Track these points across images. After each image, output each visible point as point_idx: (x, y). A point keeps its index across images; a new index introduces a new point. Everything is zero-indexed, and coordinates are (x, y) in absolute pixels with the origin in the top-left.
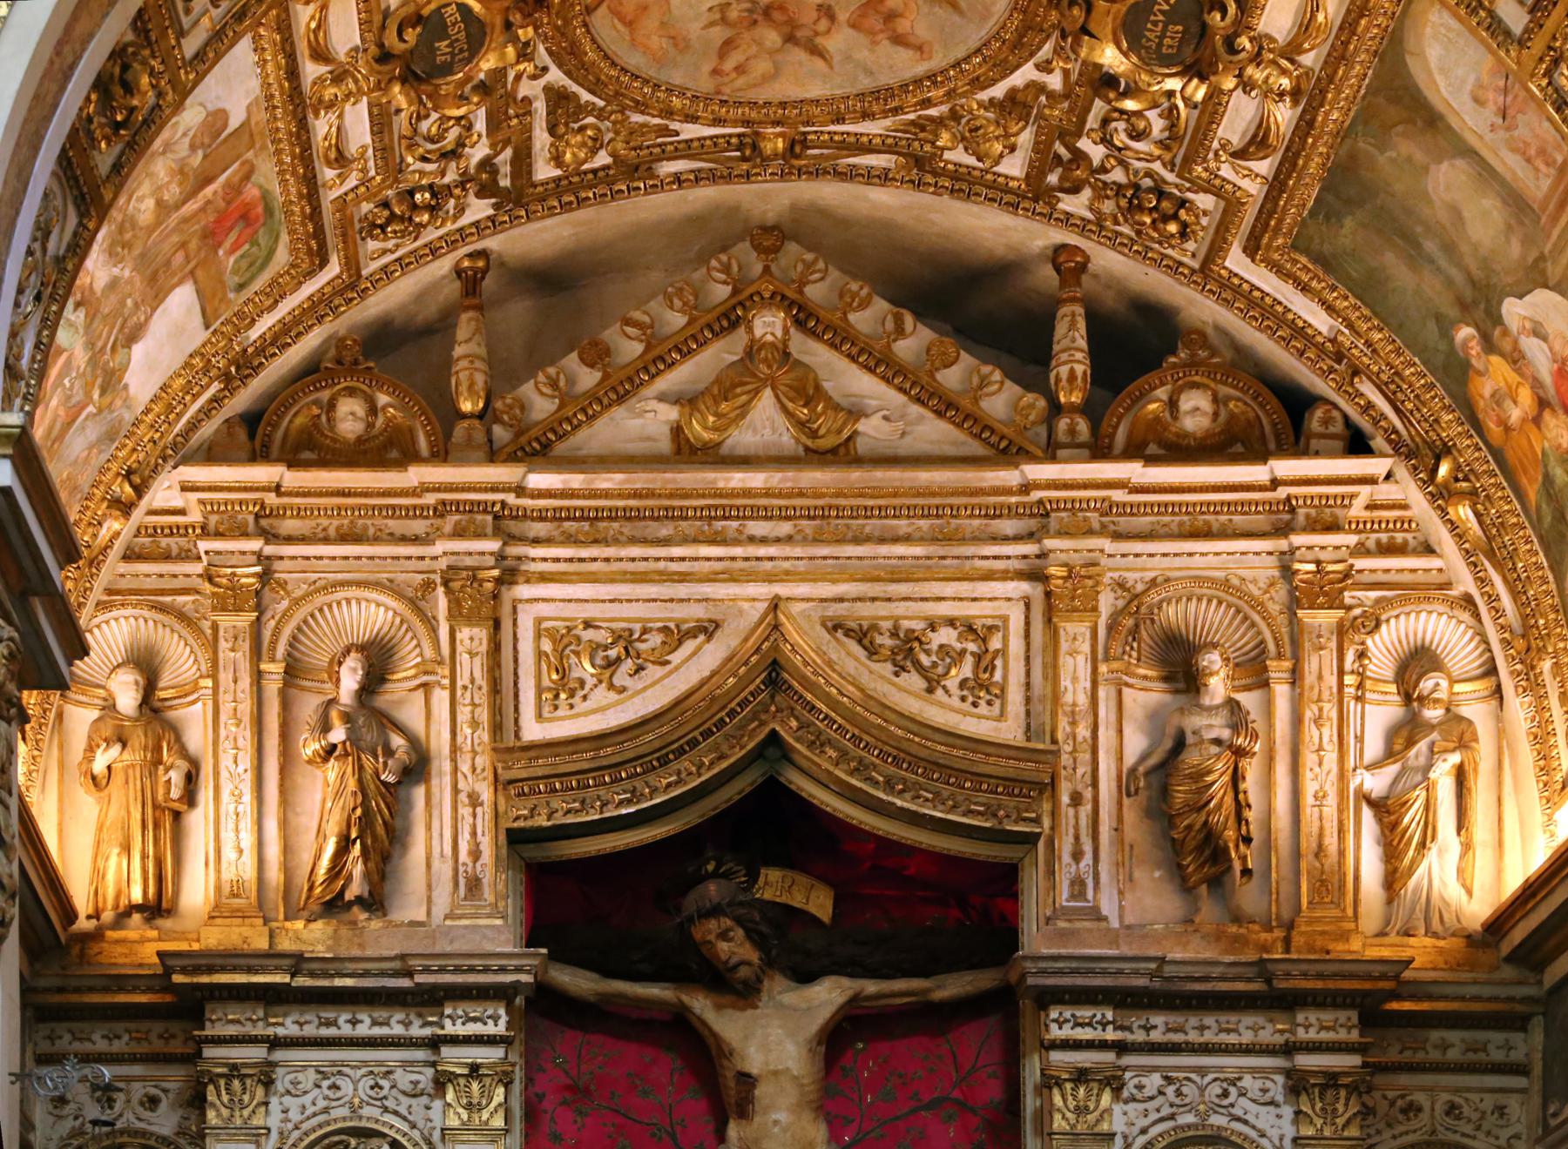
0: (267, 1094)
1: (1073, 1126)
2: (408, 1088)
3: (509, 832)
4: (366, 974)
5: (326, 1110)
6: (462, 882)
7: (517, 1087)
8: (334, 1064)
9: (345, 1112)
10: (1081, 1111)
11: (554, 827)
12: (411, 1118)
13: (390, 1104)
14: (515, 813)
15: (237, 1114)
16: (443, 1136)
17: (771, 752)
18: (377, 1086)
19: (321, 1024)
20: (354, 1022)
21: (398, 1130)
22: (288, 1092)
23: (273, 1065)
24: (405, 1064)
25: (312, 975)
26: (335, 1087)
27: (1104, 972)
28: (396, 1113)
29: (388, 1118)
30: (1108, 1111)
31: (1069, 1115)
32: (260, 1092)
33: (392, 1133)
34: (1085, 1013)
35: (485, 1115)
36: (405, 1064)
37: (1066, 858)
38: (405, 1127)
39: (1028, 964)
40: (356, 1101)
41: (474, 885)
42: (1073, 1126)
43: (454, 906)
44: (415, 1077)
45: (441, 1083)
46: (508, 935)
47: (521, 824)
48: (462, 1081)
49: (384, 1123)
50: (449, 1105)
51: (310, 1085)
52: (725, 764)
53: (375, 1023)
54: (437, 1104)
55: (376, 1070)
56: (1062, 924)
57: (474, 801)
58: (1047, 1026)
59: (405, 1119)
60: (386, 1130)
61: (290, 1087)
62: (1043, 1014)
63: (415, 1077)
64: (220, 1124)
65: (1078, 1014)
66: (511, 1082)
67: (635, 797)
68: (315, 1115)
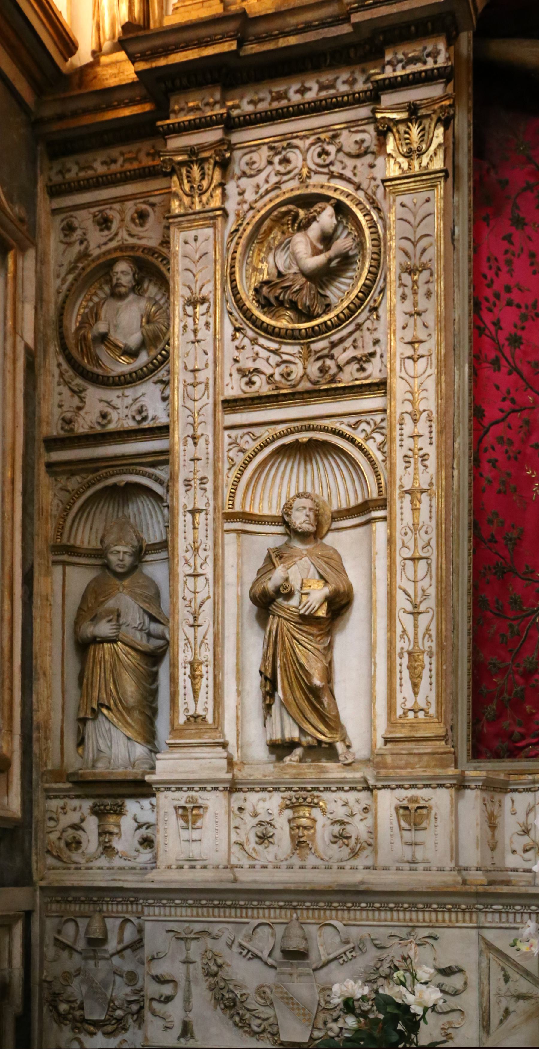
0: (224, 175)
2: (353, 149)
4: (308, 27)
5: (277, 186)
8: (285, 137)
9: (294, 184)
12: (356, 179)
13: (336, 169)
15: (197, 199)
18: (324, 152)
19: (273, 99)
20: (303, 91)
21: (343, 192)
22: (244, 174)
23: (232, 148)
24: (351, 125)
25: (259, 40)
26: (286, 161)
28: (341, 177)
29: (335, 183)
32: (217, 176)
33: (337, 195)
35: (425, 160)
36: (351, 125)
38: (349, 189)
40: (305, 171)
44: (359, 137)
45: (382, 135)
49: (329, 188)
51: (264, 162)
53: (322, 88)
55: (323, 136)
59: (349, 181)
60: (330, 193)
61: (246, 169)
63: (359, 137)
64: (182, 211)
68: (267, 192)
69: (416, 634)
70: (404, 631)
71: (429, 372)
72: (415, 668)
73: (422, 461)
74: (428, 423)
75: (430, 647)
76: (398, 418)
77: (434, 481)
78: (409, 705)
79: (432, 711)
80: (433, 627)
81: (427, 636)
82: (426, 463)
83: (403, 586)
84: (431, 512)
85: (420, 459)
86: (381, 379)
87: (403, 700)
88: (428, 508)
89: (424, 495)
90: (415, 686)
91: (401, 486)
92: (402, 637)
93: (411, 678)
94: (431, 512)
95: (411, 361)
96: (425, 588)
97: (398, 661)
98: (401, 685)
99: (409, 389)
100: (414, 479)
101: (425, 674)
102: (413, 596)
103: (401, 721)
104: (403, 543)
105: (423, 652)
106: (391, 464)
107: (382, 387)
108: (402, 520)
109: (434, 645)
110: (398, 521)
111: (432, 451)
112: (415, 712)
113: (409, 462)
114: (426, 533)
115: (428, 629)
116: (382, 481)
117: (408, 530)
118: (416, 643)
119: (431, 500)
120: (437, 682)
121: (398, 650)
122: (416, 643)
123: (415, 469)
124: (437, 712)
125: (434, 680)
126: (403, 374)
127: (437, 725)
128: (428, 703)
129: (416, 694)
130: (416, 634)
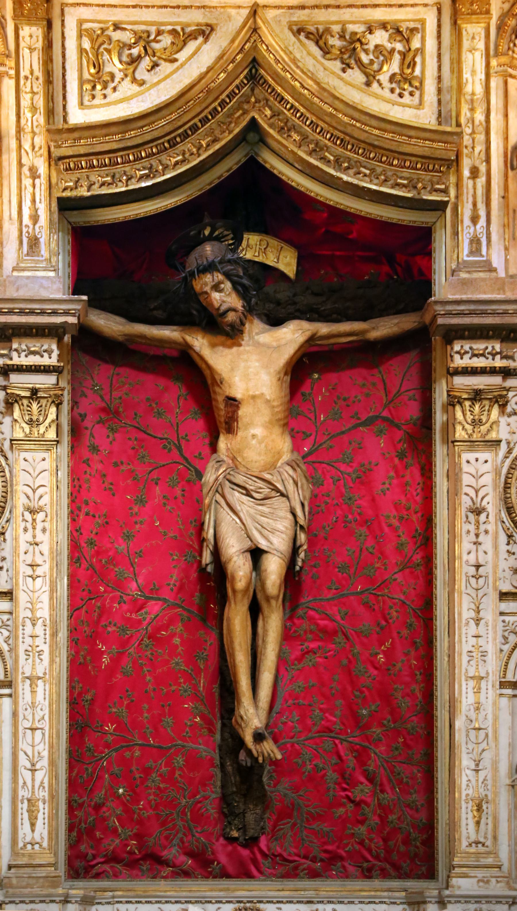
1: (470, 435)
3: (60, 200)
6: (25, 240)
7: (66, 407)
10: (476, 423)
11: (93, 197)
14: (64, 185)
16: (12, 445)
17: (252, 137)
27: (494, 313)
30: (496, 422)
31: (467, 427)
34: (479, 346)
37: (467, 221)
39: (438, 308)
41: (34, 243)
42: (470, 435)
43: (20, 260)
46: (58, 285)
47: (67, 194)
48: (25, 402)
50: (16, 421)
52: (217, 146)
54: (7, 420)
56: (463, 275)
57: (34, 174)
58: (452, 356)
62: (449, 347)
65: (475, 346)
66: (61, 403)
67: (152, 173)
69: (33, 786)
70: (25, 783)
71: (44, 589)
72: (33, 812)
73: (39, 655)
74: (44, 627)
75: (44, 796)
76: (21, 621)
77: (47, 671)
78: (28, 839)
79: (45, 844)
80: (46, 781)
81: (41, 788)
82: (41, 657)
83: (24, 749)
84: (45, 694)
85: (37, 654)
86: (9, 590)
87: (24, 836)
88: (43, 692)
89: (40, 681)
90: (33, 825)
91: (23, 673)
92: (23, 787)
93: (30, 819)
94: (45, 694)
95: (31, 579)
96: (40, 751)
97: (20, 805)
98: (22, 824)
99: (29, 600)
100: (33, 668)
101: (40, 816)
102: (31, 757)
103: (22, 851)
104: (24, 716)
105: (39, 800)
106: (16, 656)
107: (8, 595)
108: (23, 698)
109: (46, 794)
110: (20, 700)
111: (46, 648)
112: (33, 845)
113: (29, 655)
114: (41, 710)
115: (42, 783)
116: (8, 667)
117: (28, 707)
118: (33, 792)
119: (45, 685)
120: (49, 822)
121: (20, 798)
122: (33, 792)
123: (33, 661)
124: (49, 845)
125: (46, 821)
126: (25, 588)
127: (49, 855)
128: (42, 838)
129: (33, 831)
130: (33, 786)
